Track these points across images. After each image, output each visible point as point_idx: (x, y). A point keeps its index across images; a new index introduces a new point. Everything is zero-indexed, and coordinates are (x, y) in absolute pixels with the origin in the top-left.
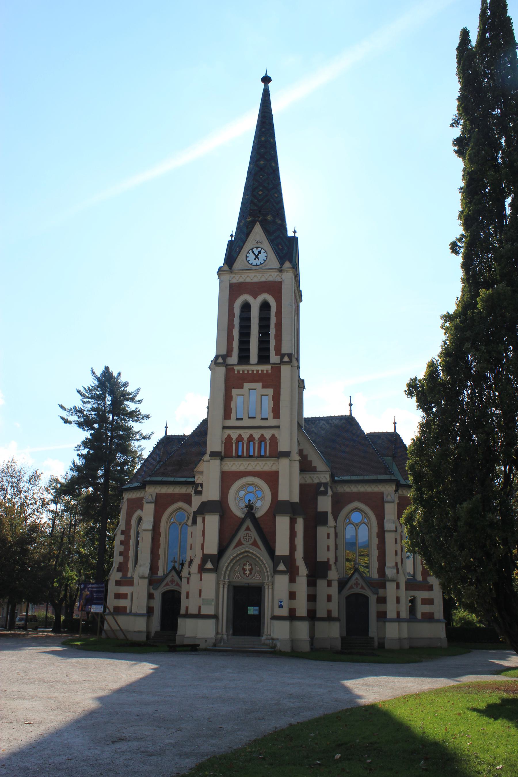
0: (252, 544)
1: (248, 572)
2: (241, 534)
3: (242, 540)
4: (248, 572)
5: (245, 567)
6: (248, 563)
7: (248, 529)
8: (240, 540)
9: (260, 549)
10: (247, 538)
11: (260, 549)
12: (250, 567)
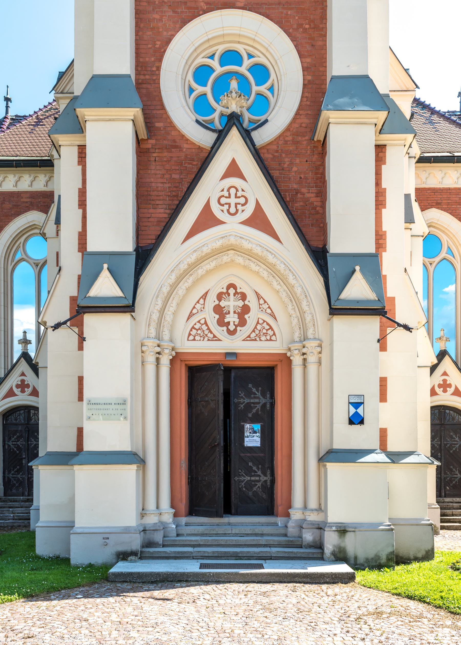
0: (246, 223)
1: (232, 318)
2: (211, 186)
3: (215, 209)
4: (232, 318)
5: (223, 304)
6: (232, 291)
7: (233, 170)
8: (207, 206)
9: (276, 237)
10: (233, 201)
11: (276, 237)
12: (241, 303)
